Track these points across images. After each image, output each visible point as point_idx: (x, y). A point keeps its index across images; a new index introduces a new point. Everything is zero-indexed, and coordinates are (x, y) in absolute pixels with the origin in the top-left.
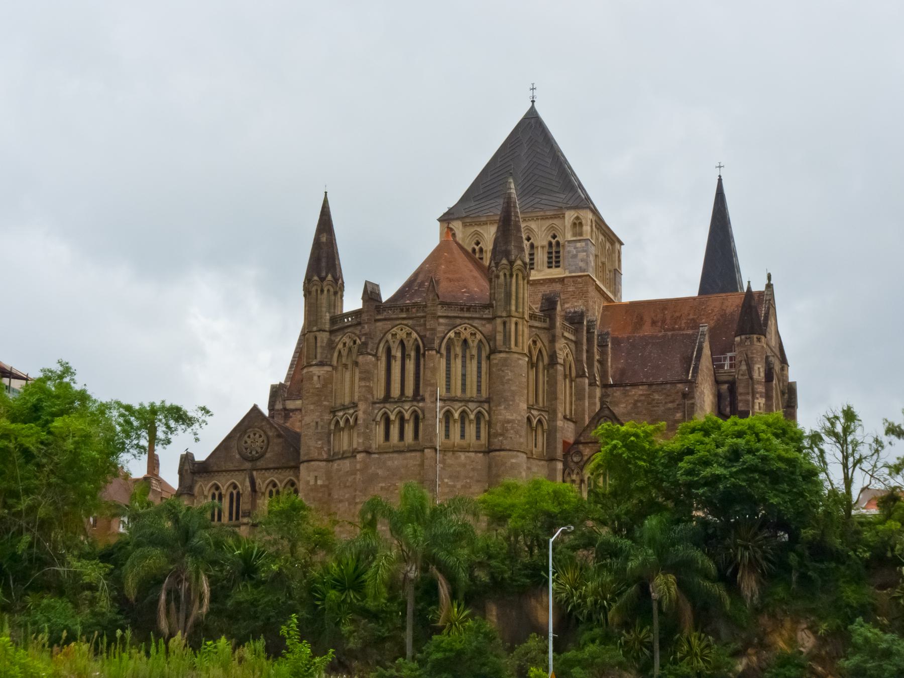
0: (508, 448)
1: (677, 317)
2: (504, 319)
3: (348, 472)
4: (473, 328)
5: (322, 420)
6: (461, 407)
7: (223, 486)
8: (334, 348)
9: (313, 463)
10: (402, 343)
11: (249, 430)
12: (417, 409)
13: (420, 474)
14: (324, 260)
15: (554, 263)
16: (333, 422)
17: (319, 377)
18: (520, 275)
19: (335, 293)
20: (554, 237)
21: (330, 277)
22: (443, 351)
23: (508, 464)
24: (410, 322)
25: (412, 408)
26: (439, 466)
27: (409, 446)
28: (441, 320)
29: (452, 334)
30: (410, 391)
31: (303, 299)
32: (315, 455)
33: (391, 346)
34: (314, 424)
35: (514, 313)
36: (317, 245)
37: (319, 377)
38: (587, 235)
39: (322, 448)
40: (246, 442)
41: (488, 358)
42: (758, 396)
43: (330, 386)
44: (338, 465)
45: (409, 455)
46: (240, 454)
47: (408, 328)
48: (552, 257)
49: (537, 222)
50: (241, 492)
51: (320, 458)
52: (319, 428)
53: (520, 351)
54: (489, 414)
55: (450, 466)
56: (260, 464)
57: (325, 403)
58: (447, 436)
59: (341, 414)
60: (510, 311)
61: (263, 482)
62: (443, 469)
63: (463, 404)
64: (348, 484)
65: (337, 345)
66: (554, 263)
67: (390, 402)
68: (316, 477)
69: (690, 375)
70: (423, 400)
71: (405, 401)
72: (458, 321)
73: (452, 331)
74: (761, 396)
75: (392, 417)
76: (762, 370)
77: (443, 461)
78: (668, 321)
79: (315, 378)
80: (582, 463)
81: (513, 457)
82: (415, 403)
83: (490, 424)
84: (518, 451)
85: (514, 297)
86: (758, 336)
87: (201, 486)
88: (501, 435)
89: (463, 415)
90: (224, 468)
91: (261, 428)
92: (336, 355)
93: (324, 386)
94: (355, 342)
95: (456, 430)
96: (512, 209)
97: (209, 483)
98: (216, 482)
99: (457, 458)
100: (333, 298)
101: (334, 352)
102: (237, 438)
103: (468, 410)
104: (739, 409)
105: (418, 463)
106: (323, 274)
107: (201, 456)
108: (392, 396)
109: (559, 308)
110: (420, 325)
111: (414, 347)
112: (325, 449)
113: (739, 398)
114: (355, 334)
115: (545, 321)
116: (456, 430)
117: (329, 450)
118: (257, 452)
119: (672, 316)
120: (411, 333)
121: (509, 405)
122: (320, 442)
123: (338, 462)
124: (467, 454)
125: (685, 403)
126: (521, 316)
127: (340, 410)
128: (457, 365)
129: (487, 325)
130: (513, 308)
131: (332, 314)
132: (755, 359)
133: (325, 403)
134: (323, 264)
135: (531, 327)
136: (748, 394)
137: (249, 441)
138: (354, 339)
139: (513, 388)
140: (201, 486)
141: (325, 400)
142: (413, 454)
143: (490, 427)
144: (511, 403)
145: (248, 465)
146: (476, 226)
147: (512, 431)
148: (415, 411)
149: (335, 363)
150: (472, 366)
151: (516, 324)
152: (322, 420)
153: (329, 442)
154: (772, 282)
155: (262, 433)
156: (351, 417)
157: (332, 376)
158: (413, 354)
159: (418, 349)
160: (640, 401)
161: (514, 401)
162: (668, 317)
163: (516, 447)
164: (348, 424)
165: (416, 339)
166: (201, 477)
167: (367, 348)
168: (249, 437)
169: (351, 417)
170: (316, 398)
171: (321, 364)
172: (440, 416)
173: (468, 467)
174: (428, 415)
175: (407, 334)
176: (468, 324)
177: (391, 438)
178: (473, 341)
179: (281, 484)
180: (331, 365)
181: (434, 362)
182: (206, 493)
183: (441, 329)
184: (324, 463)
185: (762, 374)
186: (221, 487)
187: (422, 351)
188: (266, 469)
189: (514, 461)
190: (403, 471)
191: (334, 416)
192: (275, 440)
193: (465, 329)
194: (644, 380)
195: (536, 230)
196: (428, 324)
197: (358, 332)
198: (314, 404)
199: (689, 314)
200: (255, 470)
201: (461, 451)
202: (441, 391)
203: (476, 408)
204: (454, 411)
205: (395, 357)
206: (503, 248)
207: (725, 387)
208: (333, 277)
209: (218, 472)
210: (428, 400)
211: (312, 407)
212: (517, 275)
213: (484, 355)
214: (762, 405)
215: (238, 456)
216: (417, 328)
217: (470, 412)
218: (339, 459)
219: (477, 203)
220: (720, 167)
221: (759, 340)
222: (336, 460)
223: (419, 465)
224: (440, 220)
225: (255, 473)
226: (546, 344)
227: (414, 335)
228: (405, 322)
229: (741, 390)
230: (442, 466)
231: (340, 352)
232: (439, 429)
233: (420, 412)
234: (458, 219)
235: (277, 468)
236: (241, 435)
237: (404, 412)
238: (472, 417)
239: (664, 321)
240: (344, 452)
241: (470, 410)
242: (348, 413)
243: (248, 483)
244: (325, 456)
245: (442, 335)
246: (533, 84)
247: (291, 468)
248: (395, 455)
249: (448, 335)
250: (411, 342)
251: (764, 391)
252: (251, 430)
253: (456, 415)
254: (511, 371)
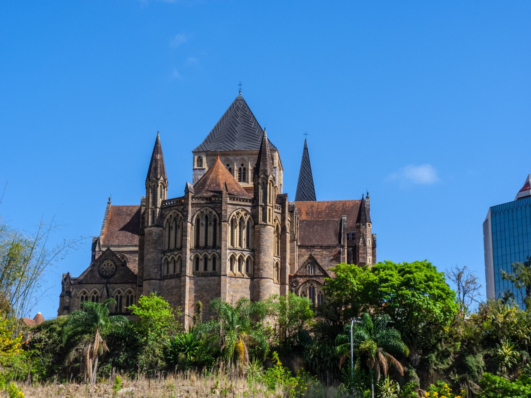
0: (265, 277)
1: (320, 211)
3: (173, 287)
5: (158, 257)
7: (89, 292)
8: (165, 218)
9: (152, 281)
10: (206, 217)
11: (104, 262)
12: (215, 253)
13: (217, 289)
14: (159, 169)
15: (242, 179)
16: (164, 259)
17: (156, 233)
18: (271, 184)
19: (164, 188)
20: (242, 165)
21: (162, 179)
22: (230, 223)
23: (266, 286)
24: (212, 205)
25: (212, 253)
26: (228, 285)
27: (211, 273)
28: (229, 206)
29: (235, 213)
30: (210, 243)
31: (145, 189)
32: (154, 277)
33: (200, 218)
34: (153, 259)
35: (268, 204)
36: (153, 159)
37: (156, 233)
38: (276, 165)
39: (157, 273)
40: (103, 268)
41: (253, 227)
42: (368, 255)
43: (162, 238)
44: (167, 282)
45: (211, 278)
46: (99, 274)
47: (210, 209)
48: (243, 176)
49: (248, 156)
50: (99, 296)
51: (156, 278)
52: (156, 261)
53: (272, 225)
55: (234, 285)
56: (111, 280)
57: (159, 248)
58: (232, 269)
59: (169, 254)
60: (266, 202)
61: (113, 291)
62: (230, 287)
63: (241, 252)
64: (174, 293)
65: (166, 215)
66: (242, 179)
67: (200, 249)
68: (154, 289)
69: (342, 242)
70: (220, 248)
71: (209, 249)
72: (238, 207)
74: (370, 255)
75: (201, 257)
76: (371, 241)
77: (230, 283)
78: (315, 213)
79: (154, 234)
80: (298, 287)
81: (267, 282)
82: (215, 250)
84: (270, 279)
85: (268, 195)
86: (369, 223)
87: (75, 291)
88: (262, 270)
89: (241, 258)
90: (89, 282)
91: (112, 260)
92: (165, 221)
93: (159, 238)
94: (178, 215)
95: (236, 265)
96: (267, 148)
97: (80, 290)
98: (85, 290)
99: (237, 281)
100: (163, 190)
101: (164, 220)
102: (97, 266)
104: (360, 261)
105: (216, 283)
106: (159, 177)
107: (75, 275)
108: (200, 246)
109: (287, 203)
110: (218, 208)
111: (213, 220)
112: (159, 273)
113: (360, 256)
114: (179, 211)
115: (280, 209)
116: (236, 265)
117: (161, 274)
118: (109, 274)
119: (317, 211)
120: (212, 212)
121: (266, 253)
122: (156, 270)
123: (167, 280)
124: (242, 279)
125: (340, 257)
126: (272, 205)
127: (169, 252)
128: (237, 231)
130: (268, 201)
131: (163, 199)
132: (367, 235)
133: (159, 248)
134: (159, 171)
135: (275, 212)
136: (364, 253)
137: (105, 268)
138: (178, 213)
139: (268, 244)
140: (75, 291)
141: (159, 247)
142: (213, 278)
143: (254, 264)
144: (267, 252)
145: (105, 281)
146: (213, 157)
147: (267, 268)
148: (214, 254)
149: (164, 226)
150: (244, 232)
151: (269, 210)
152: (158, 257)
153: (161, 269)
154: (369, 196)
155: (112, 264)
156: (176, 256)
157: (163, 234)
158: (212, 223)
159: (215, 220)
160: (316, 255)
161: (268, 251)
162: (315, 211)
163: (270, 277)
164: (173, 260)
165: (215, 215)
166: (75, 287)
167: (187, 219)
168: (105, 265)
169: (176, 256)
170: (155, 245)
171: (157, 226)
172: (229, 258)
173: (243, 286)
174: (223, 257)
175: (210, 212)
177: (199, 269)
178: (246, 218)
179: (124, 292)
180: (162, 227)
181: (226, 228)
182: (78, 296)
183: (229, 210)
184: (159, 281)
185: (371, 244)
186: (88, 293)
187: (218, 222)
188: (115, 283)
189: (268, 284)
190: (207, 287)
191: (164, 255)
192: (121, 268)
193: (242, 211)
194: (316, 244)
195: (247, 160)
196: (223, 207)
197: (180, 210)
198: (153, 248)
199: (326, 211)
200: (108, 283)
201: (239, 278)
202: (229, 245)
205: (202, 224)
206: (263, 168)
207: (351, 249)
208: (164, 178)
209: (86, 284)
210: (223, 249)
211: (152, 250)
212: (270, 183)
213: (250, 226)
214: (370, 260)
215: (98, 276)
216: (216, 209)
218: (167, 279)
219: (216, 143)
220: (306, 134)
221: (369, 225)
222: (166, 279)
223: (217, 284)
224: (193, 152)
225: (108, 285)
226: (280, 222)
227: (214, 213)
228: (209, 205)
229: (360, 251)
230: (229, 285)
231: (168, 220)
232: (228, 263)
233: (217, 255)
234: (204, 151)
235: (122, 283)
236: (100, 264)
237: (208, 255)
238: (245, 259)
239: (313, 213)
240: (170, 275)
242: (174, 254)
243: (105, 291)
244: (159, 278)
245: (230, 214)
246: (240, 82)
247: (130, 283)
248: (203, 278)
250: (212, 216)
251: (371, 252)
252: (106, 261)
253: (237, 258)
254: (267, 235)
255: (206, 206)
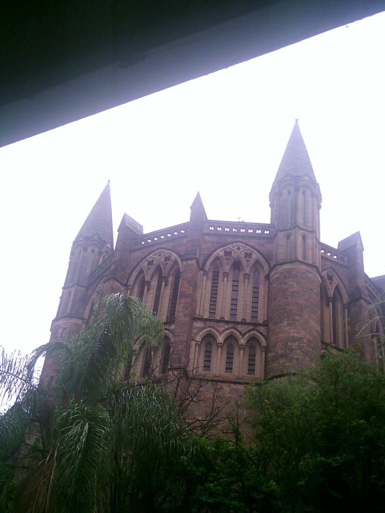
2: (288, 231)
4: (248, 247)
6: (227, 329)
54: (267, 339)
73: (222, 249)
83: (267, 350)
103: (238, 334)
129: (266, 245)
176: (242, 242)
203: (249, 331)
204: (217, 333)
217: (241, 337)
241: (241, 333)
249: (216, 253)
255: (158, 249)
